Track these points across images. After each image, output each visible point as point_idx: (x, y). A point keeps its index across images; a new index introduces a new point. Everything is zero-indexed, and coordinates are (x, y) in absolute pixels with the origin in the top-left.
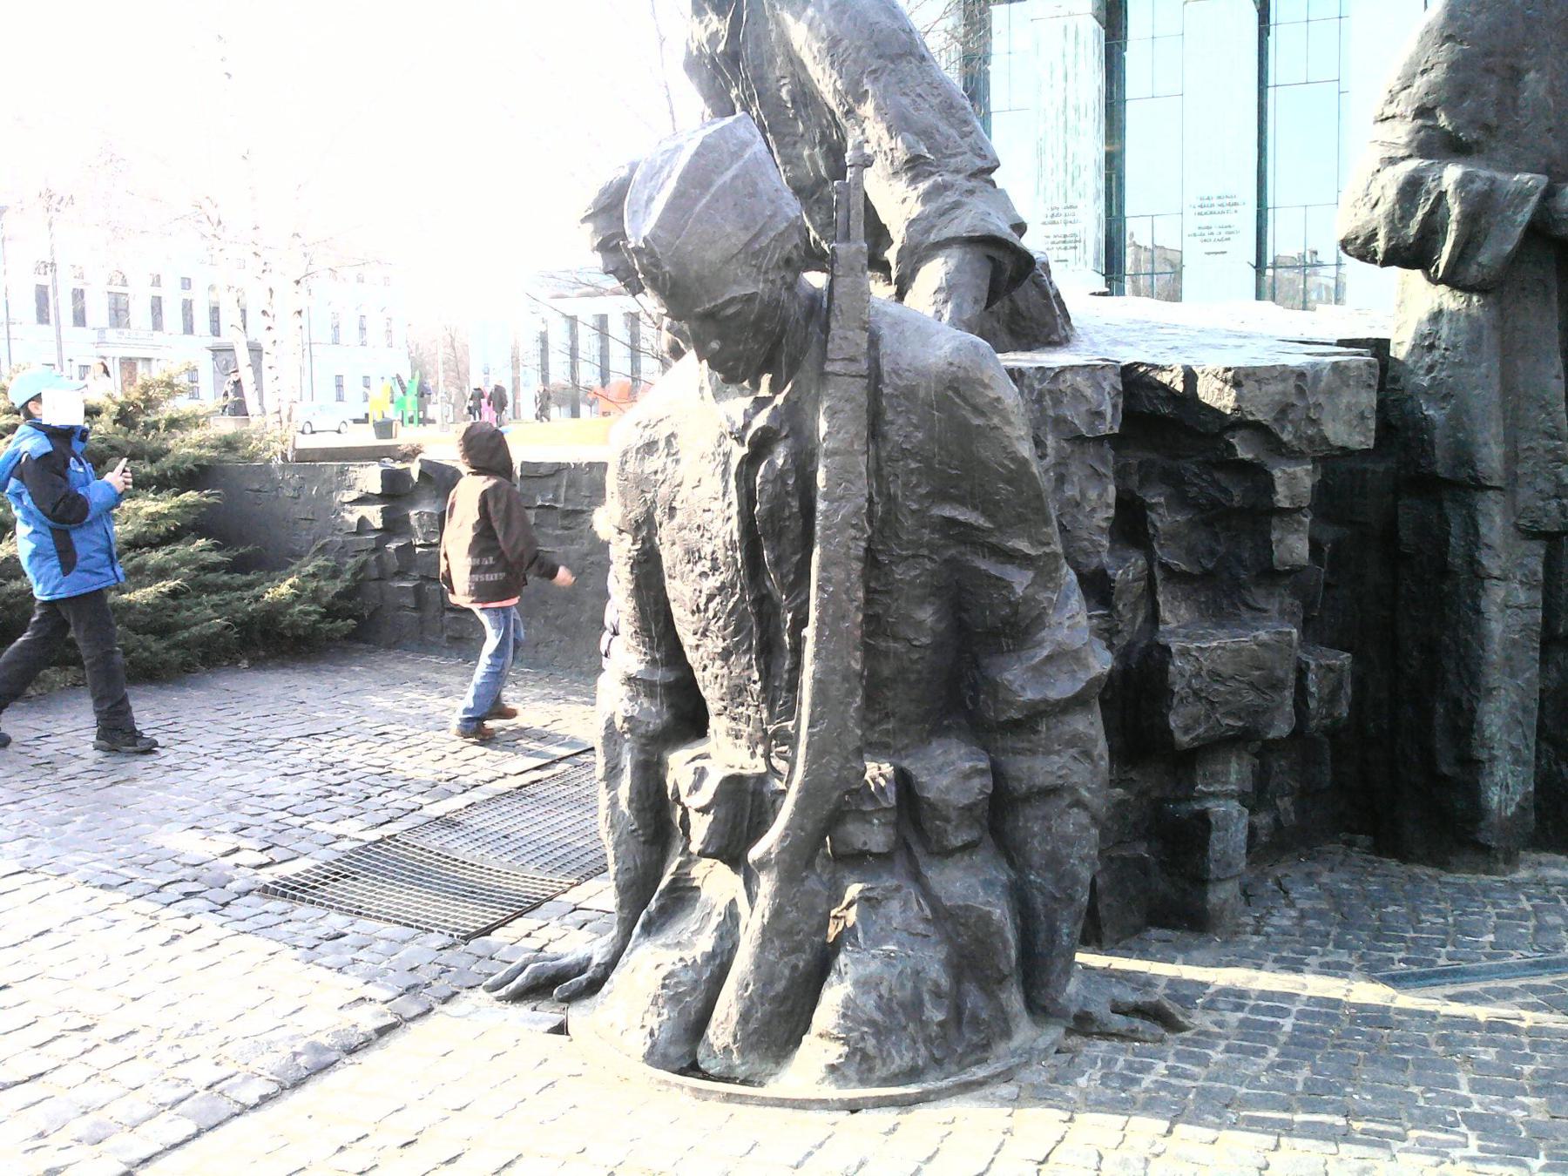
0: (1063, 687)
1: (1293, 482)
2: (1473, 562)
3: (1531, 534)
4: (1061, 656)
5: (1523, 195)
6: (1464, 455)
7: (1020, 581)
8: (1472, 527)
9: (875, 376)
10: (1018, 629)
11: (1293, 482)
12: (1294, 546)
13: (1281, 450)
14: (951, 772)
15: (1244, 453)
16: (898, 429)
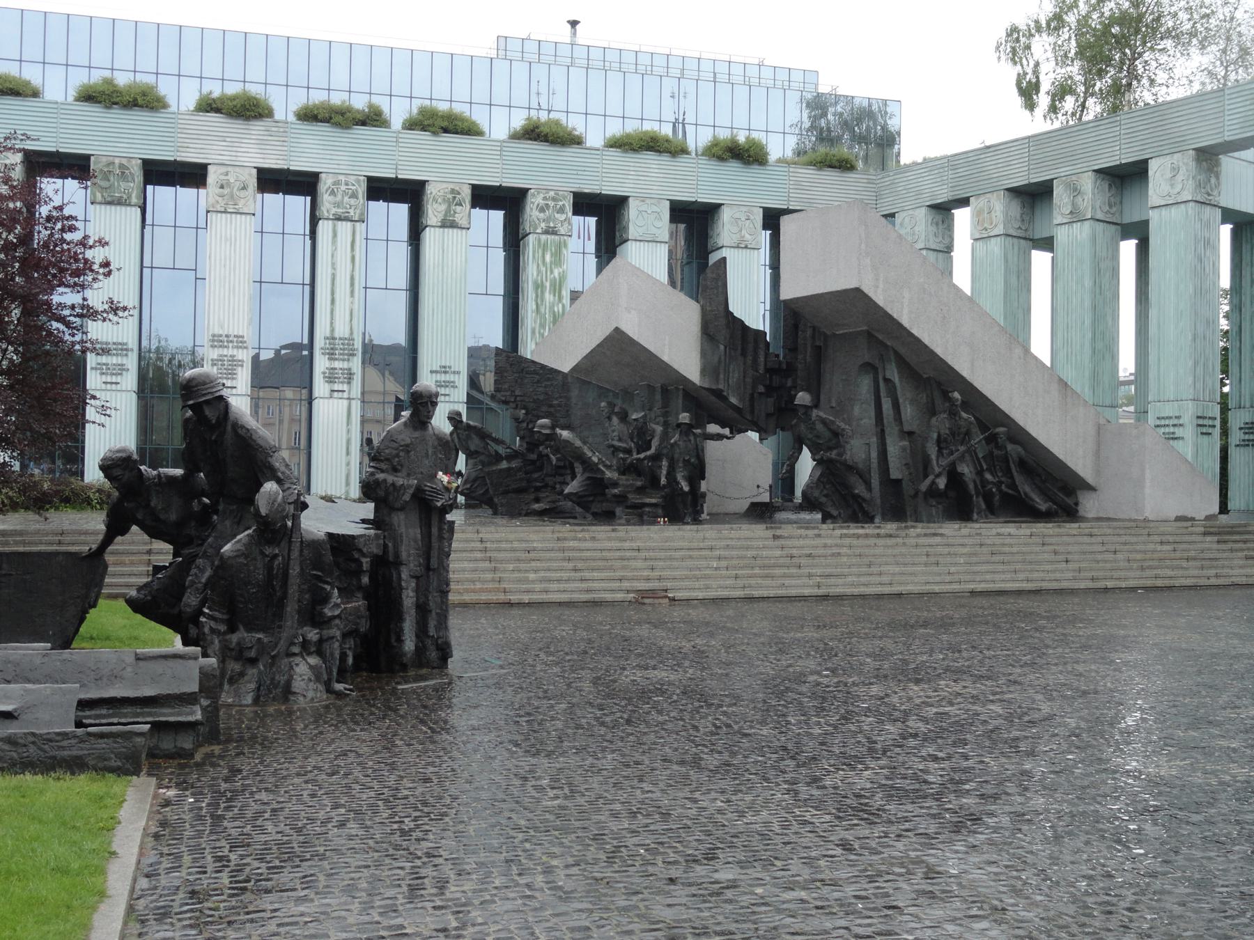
0: (337, 612)
1: (366, 562)
2: (400, 585)
3: (412, 577)
4: (337, 605)
5: (410, 486)
6: (397, 555)
7: (328, 587)
8: (400, 575)
9: (302, 542)
10: (325, 599)
11: (366, 562)
12: (365, 580)
13: (364, 555)
14: (313, 635)
15: (356, 556)
16: (306, 552)
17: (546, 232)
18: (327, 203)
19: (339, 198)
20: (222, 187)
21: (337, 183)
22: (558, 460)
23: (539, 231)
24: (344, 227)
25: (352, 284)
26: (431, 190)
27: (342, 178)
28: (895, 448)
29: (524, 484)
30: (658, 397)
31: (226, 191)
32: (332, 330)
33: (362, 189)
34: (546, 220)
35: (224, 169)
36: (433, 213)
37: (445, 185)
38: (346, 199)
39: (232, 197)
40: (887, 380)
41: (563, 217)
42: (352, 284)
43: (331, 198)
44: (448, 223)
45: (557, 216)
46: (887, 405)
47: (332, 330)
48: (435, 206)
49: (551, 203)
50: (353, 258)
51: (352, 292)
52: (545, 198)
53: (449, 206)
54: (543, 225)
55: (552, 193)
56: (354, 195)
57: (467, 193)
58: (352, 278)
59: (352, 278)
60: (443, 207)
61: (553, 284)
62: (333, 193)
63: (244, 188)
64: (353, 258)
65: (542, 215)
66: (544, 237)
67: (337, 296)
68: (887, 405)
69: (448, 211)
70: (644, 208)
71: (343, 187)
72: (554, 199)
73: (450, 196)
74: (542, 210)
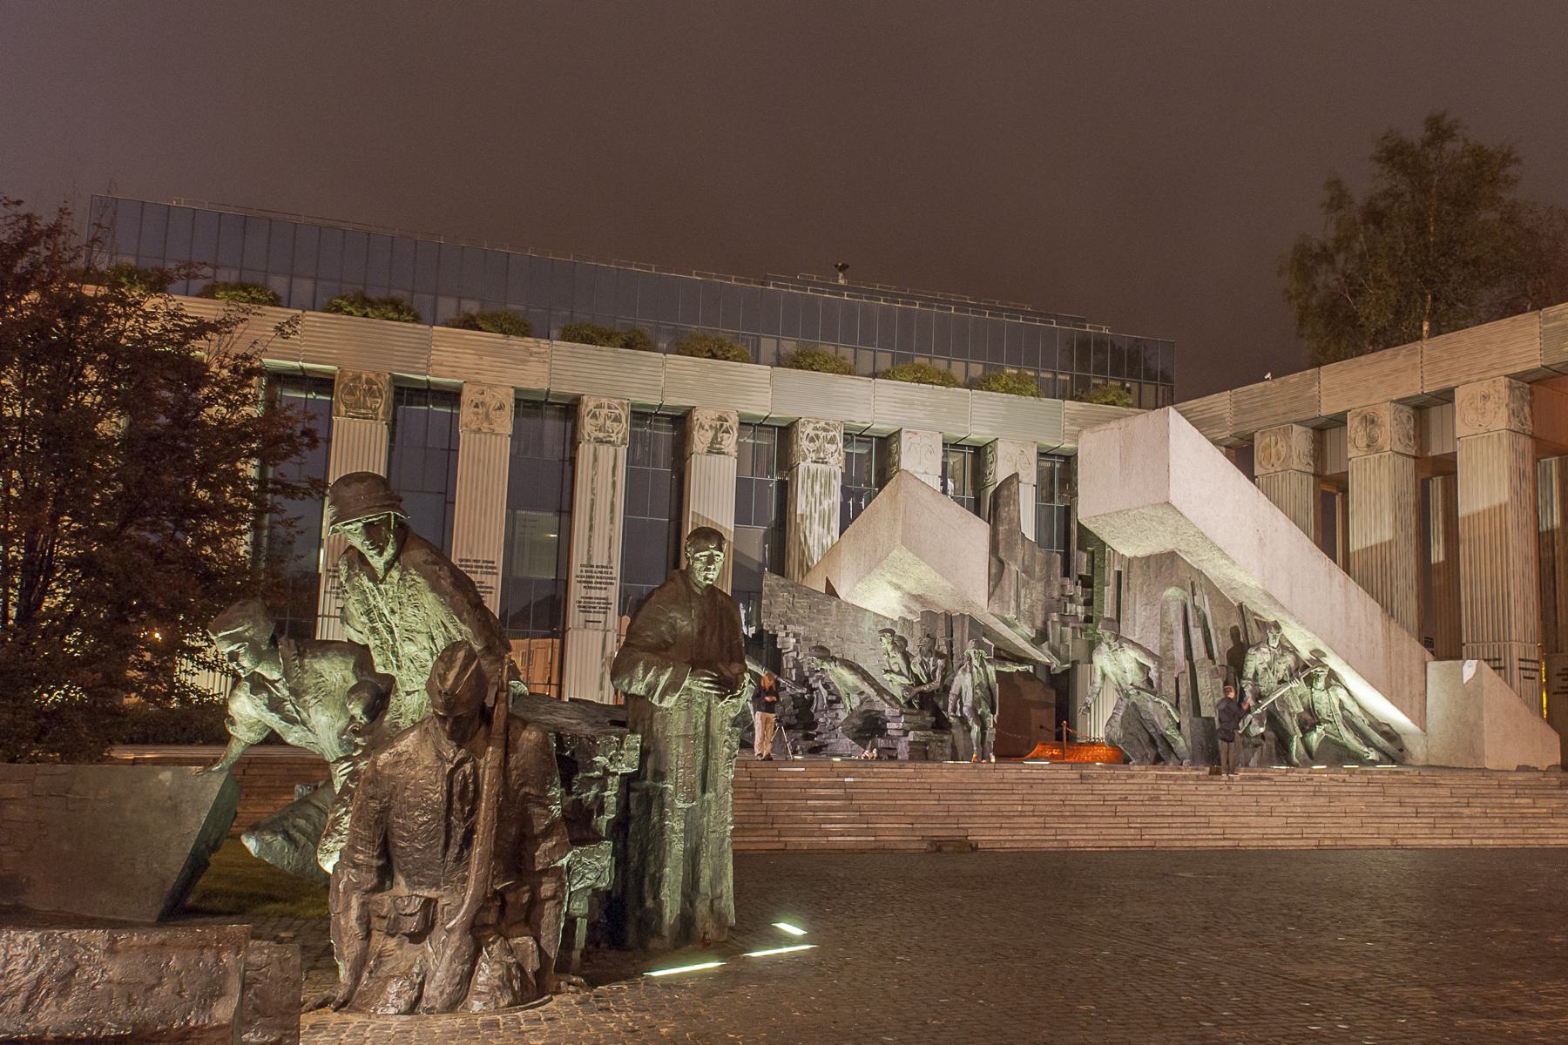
18: (588, 427)
19: (600, 421)
20: (477, 406)
21: (599, 406)
22: (830, 693)
24: (606, 452)
25: (612, 511)
27: (605, 401)
28: (1203, 682)
29: (794, 721)
30: (941, 624)
31: (480, 410)
32: (590, 558)
33: (624, 415)
34: (817, 451)
35: (479, 388)
36: (700, 440)
38: (608, 423)
39: (487, 416)
40: (1197, 609)
41: (834, 447)
42: (612, 511)
43: (593, 421)
44: (714, 449)
46: (1197, 635)
47: (590, 558)
49: (822, 434)
50: (614, 483)
51: (612, 519)
52: (815, 429)
55: (822, 424)
56: (617, 419)
57: (733, 421)
58: (612, 504)
59: (612, 504)
60: (711, 434)
61: (822, 517)
62: (594, 416)
63: (501, 408)
64: (614, 483)
67: (596, 522)
68: (1197, 635)
69: (714, 440)
71: (606, 411)
72: (825, 430)
74: (812, 440)
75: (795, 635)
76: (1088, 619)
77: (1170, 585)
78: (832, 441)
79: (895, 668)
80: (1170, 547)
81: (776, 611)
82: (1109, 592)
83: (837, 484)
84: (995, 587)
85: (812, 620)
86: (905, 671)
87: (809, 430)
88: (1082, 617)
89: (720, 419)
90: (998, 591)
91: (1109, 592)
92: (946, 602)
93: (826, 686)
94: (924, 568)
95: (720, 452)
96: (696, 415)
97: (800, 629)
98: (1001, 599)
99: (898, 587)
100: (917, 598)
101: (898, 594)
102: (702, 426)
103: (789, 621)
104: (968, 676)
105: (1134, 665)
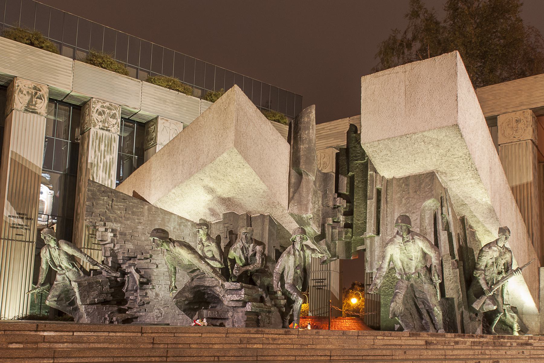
17: (102, 129)
22: (141, 276)
23: (97, 127)
26: (19, 84)
34: (104, 122)
37: (29, 82)
41: (115, 121)
44: (30, 109)
45: (111, 120)
48: (21, 95)
53: (32, 98)
54: (100, 124)
55: (107, 104)
57: (45, 92)
60: (28, 98)
65: (100, 117)
66: (101, 132)
69: (31, 101)
70: (167, 124)
72: (109, 108)
73: (34, 91)
74: (100, 114)
75: (113, 231)
76: (348, 226)
77: (429, 198)
78: (114, 116)
79: (209, 255)
80: (430, 168)
81: (98, 211)
82: (371, 204)
83: (115, 146)
84: (294, 193)
85: (128, 219)
86: (218, 257)
87: (98, 106)
88: (342, 224)
89: (35, 88)
90: (297, 195)
91: (371, 204)
92: (253, 205)
93: (137, 271)
94: (248, 170)
95: (34, 112)
96: (17, 83)
97: (117, 226)
98: (300, 202)
99: (211, 191)
100: (225, 201)
101: (209, 197)
102: (21, 91)
103: (108, 219)
104: (292, 258)
105: (420, 254)
